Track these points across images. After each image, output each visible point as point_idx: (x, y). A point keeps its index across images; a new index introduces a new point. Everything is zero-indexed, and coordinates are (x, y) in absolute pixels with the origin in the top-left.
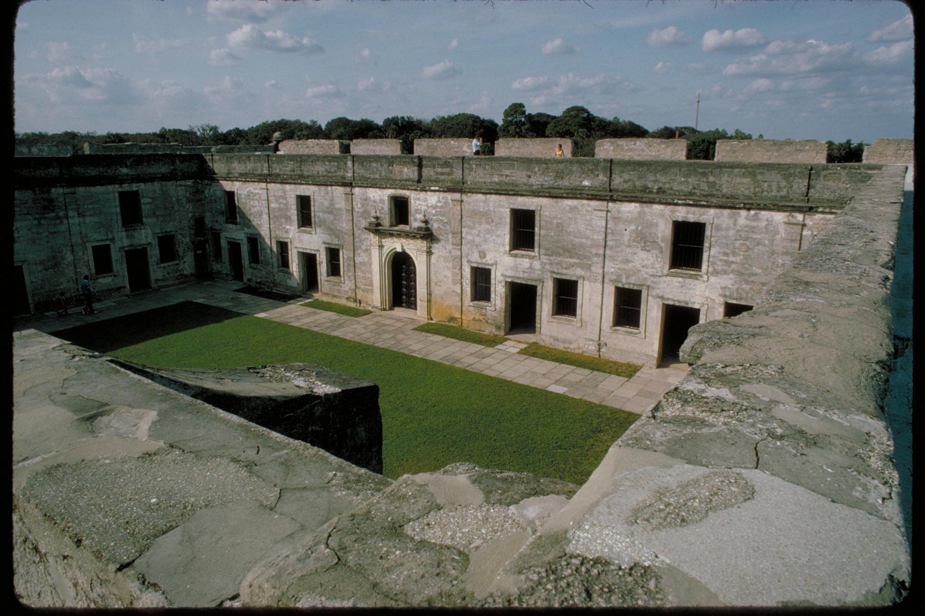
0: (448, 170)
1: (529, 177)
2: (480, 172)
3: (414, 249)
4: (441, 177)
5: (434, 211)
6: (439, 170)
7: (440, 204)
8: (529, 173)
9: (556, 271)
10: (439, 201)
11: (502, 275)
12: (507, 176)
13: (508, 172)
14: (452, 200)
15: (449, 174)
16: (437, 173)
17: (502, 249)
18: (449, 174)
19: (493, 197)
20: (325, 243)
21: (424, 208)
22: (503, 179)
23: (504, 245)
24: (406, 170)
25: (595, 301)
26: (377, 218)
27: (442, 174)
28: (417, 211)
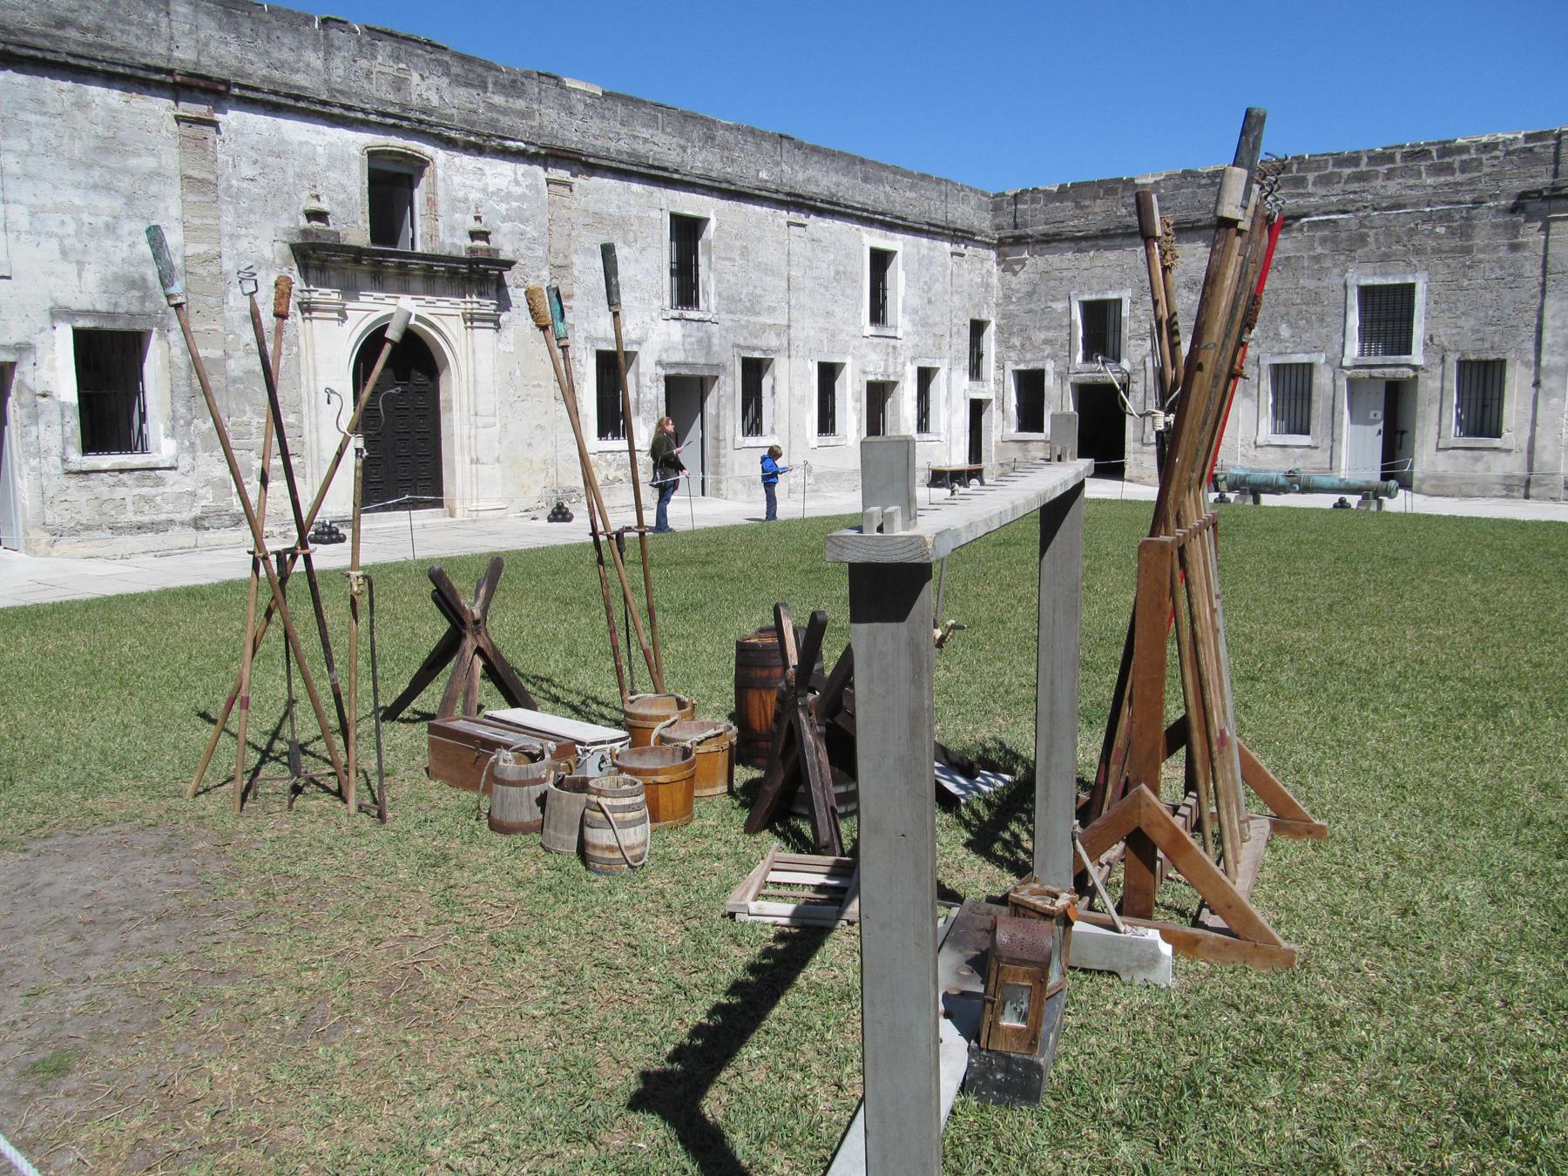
0: (520, 104)
1: (684, 149)
2: (595, 125)
3: (444, 317)
4: (505, 121)
5: (503, 208)
6: (498, 100)
7: (518, 190)
8: (682, 142)
9: (742, 342)
10: (517, 183)
11: (659, 363)
12: (646, 141)
13: (646, 133)
14: (549, 182)
15: (524, 115)
16: (492, 107)
17: (657, 303)
18: (524, 115)
19: (636, 187)
20: (59, 313)
21: (474, 196)
22: (641, 148)
23: (660, 297)
24: (415, 78)
25: (791, 392)
26: (320, 216)
27: (505, 111)
28: (454, 203)
